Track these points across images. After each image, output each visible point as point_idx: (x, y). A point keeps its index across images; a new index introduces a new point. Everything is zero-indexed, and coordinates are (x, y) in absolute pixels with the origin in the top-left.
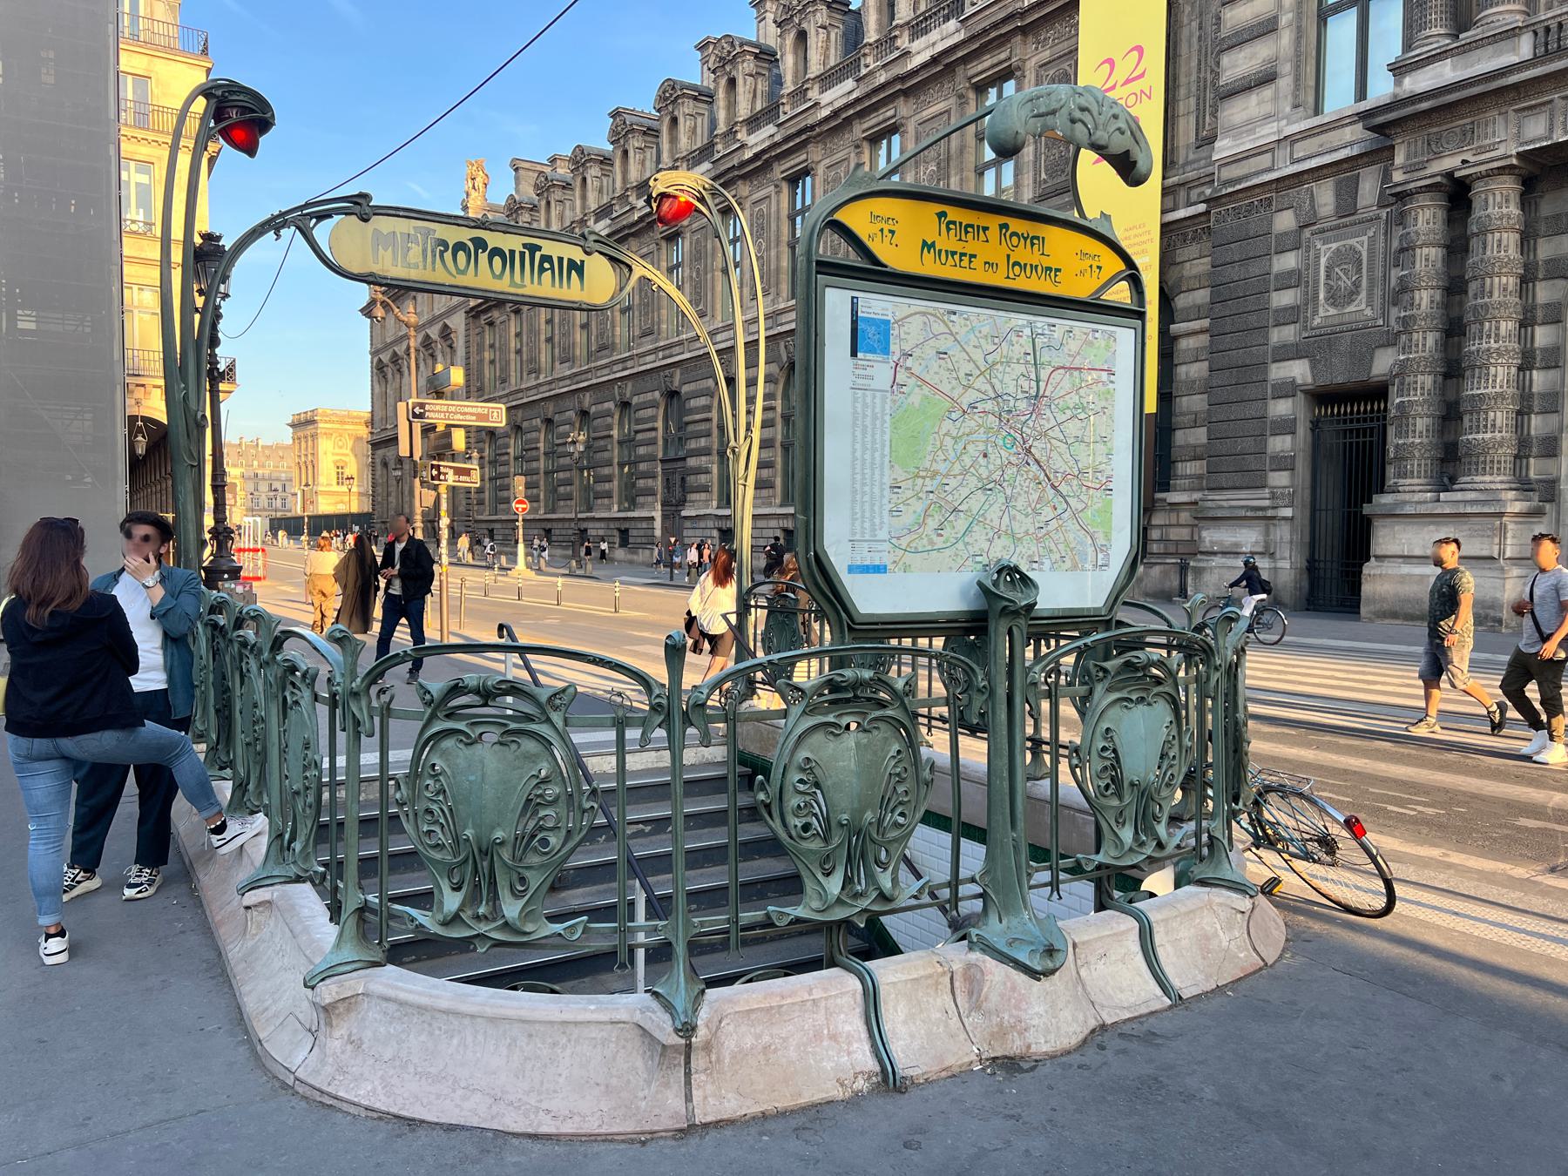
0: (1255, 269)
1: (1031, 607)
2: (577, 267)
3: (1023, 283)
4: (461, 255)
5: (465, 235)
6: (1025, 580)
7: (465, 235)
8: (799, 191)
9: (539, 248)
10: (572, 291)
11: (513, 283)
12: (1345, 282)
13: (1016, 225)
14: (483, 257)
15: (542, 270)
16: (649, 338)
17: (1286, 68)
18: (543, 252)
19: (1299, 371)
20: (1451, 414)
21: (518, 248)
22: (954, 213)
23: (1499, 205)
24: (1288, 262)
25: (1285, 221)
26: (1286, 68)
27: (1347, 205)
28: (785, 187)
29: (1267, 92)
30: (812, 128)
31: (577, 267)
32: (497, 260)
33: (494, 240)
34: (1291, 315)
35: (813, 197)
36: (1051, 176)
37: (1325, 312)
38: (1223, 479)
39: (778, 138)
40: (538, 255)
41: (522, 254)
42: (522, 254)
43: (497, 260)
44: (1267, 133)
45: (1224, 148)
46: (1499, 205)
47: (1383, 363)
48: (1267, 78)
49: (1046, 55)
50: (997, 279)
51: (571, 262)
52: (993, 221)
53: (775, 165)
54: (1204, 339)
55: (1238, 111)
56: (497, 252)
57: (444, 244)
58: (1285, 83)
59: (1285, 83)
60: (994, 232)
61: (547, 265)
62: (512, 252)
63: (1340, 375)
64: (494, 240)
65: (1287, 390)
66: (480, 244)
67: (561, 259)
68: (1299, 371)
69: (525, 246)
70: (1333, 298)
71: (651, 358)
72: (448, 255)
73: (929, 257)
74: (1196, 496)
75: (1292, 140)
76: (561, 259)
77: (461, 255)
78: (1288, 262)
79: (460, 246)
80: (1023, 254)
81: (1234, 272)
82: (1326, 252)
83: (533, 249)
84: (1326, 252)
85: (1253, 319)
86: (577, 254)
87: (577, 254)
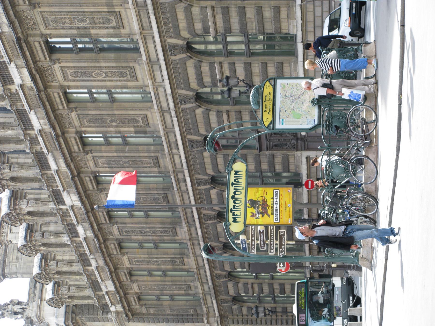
1: (317, 99)
2: (237, 172)
3: (272, 98)
4: (236, 202)
5: (231, 201)
6: (313, 99)
7: (231, 201)
8: (58, 46)
9: (232, 182)
10: (243, 174)
11: (242, 189)
13: (264, 100)
14: (236, 196)
15: (238, 182)
16: (161, 161)
18: (233, 181)
21: (233, 188)
22: (264, 110)
28: (55, 56)
30: (18, 39)
31: (237, 172)
32: (237, 193)
33: (232, 194)
35: (66, 37)
39: (21, 62)
40: (234, 183)
41: (235, 187)
42: (235, 187)
43: (237, 193)
50: (272, 102)
51: (235, 174)
52: (264, 103)
53: (40, 64)
56: (235, 193)
57: (234, 206)
60: (266, 103)
61: (237, 180)
62: (234, 189)
64: (232, 194)
66: (233, 197)
67: (235, 177)
69: (232, 186)
71: (176, 158)
72: (237, 205)
73: (270, 113)
76: (235, 177)
77: (236, 202)
79: (234, 202)
80: (268, 98)
83: (233, 184)
86: (233, 173)
87: (233, 173)
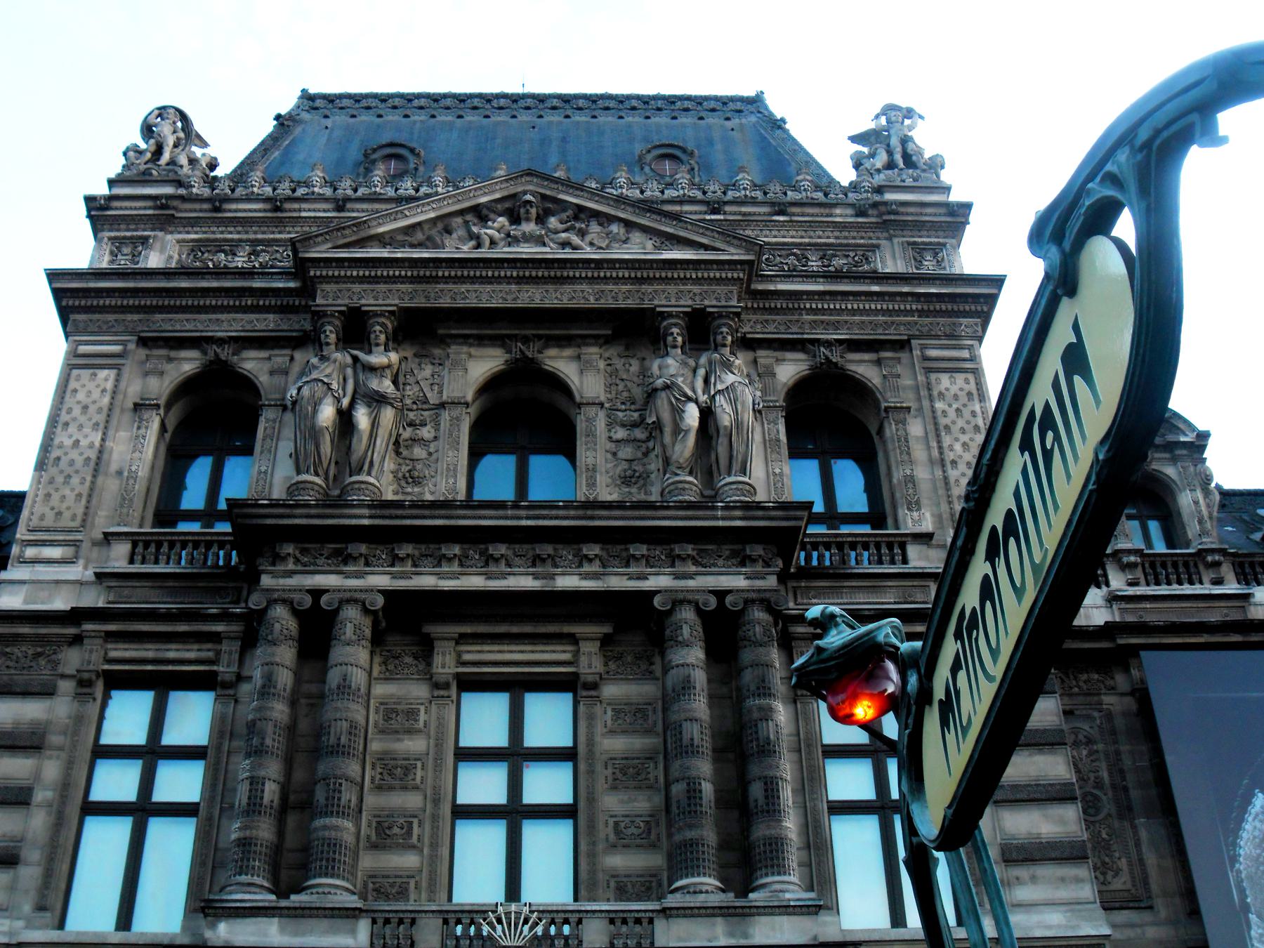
59: (29, 874)
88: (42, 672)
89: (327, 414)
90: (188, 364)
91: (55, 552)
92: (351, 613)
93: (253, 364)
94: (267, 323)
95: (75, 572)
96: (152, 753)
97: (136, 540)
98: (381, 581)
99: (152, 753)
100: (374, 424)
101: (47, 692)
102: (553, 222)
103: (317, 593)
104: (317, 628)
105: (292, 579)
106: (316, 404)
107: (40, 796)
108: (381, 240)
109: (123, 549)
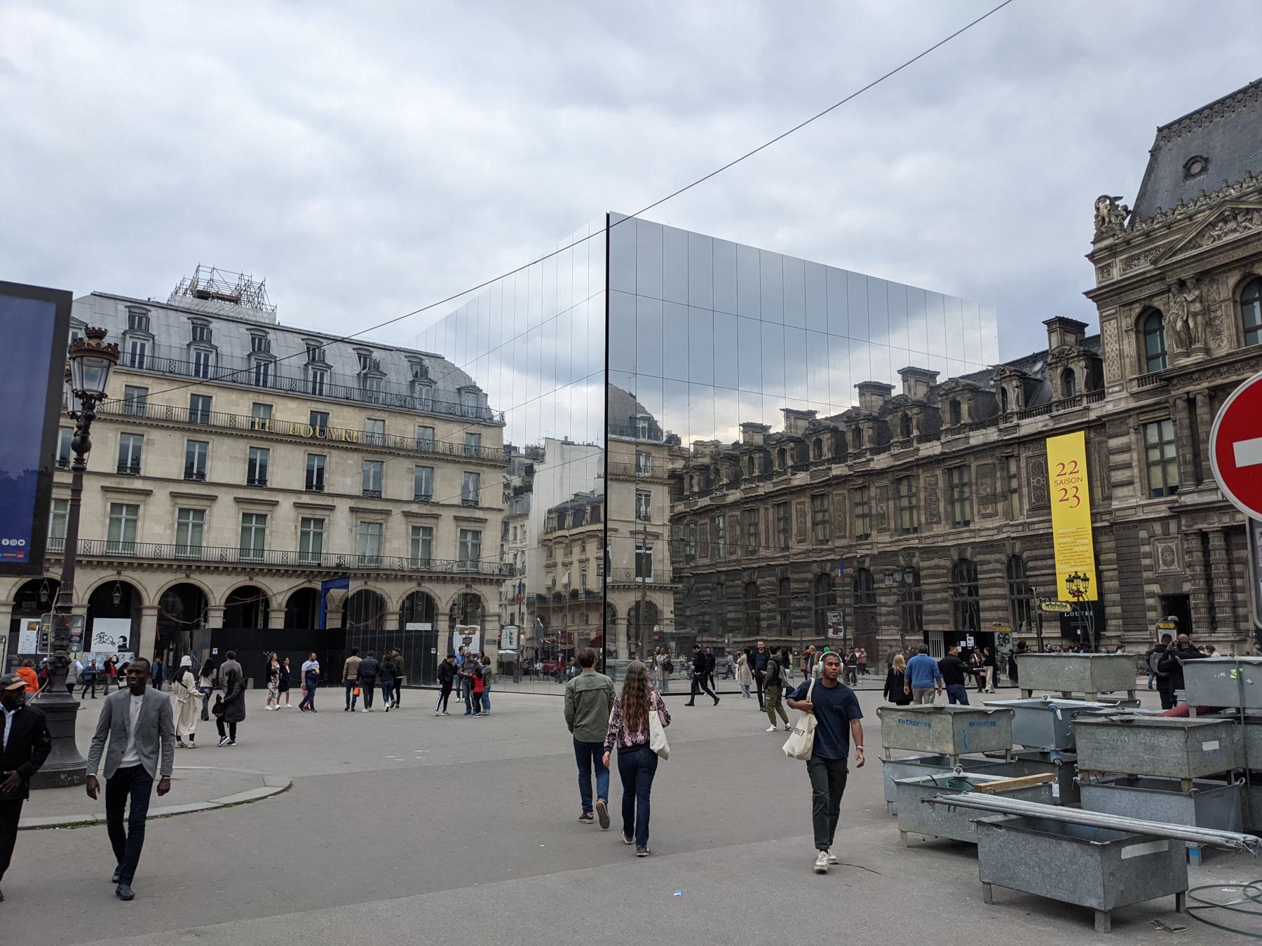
0: (1133, 550)
12: (1169, 558)
17: (1137, 480)
19: (1155, 588)
20: (1211, 608)
23: (1216, 542)
24: (1146, 549)
25: (1143, 534)
26: (1137, 480)
27: (1166, 532)
29: (1131, 488)
34: (1149, 568)
36: (1037, 501)
37: (1163, 568)
38: (1130, 627)
44: (1133, 502)
45: (1116, 504)
46: (1216, 542)
47: (1187, 587)
48: (1131, 483)
49: (1030, 454)
54: (1116, 573)
55: (1120, 492)
58: (1137, 485)
63: (1171, 591)
65: (1152, 595)
68: (1155, 588)
70: (1165, 563)
74: (1118, 633)
75: (1143, 506)
78: (1146, 549)
81: (1125, 550)
82: (1160, 547)
84: (1160, 547)
85: (1135, 568)
88: (1124, 428)
89: (1179, 324)
90: (1137, 309)
91: (1117, 389)
92: (1199, 398)
93: (1158, 303)
94: (1155, 288)
95: (1124, 394)
96: (1161, 445)
97: (1138, 379)
98: (1206, 385)
99: (1161, 445)
100: (1195, 323)
101: (1128, 433)
102: (1240, 218)
103: (1188, 393)
104: (1191, 402)
105: (1179, 391)
106: (1175, 322)
107: (1135, 464)
108: (1181, 250)
109: (1135, 383)
